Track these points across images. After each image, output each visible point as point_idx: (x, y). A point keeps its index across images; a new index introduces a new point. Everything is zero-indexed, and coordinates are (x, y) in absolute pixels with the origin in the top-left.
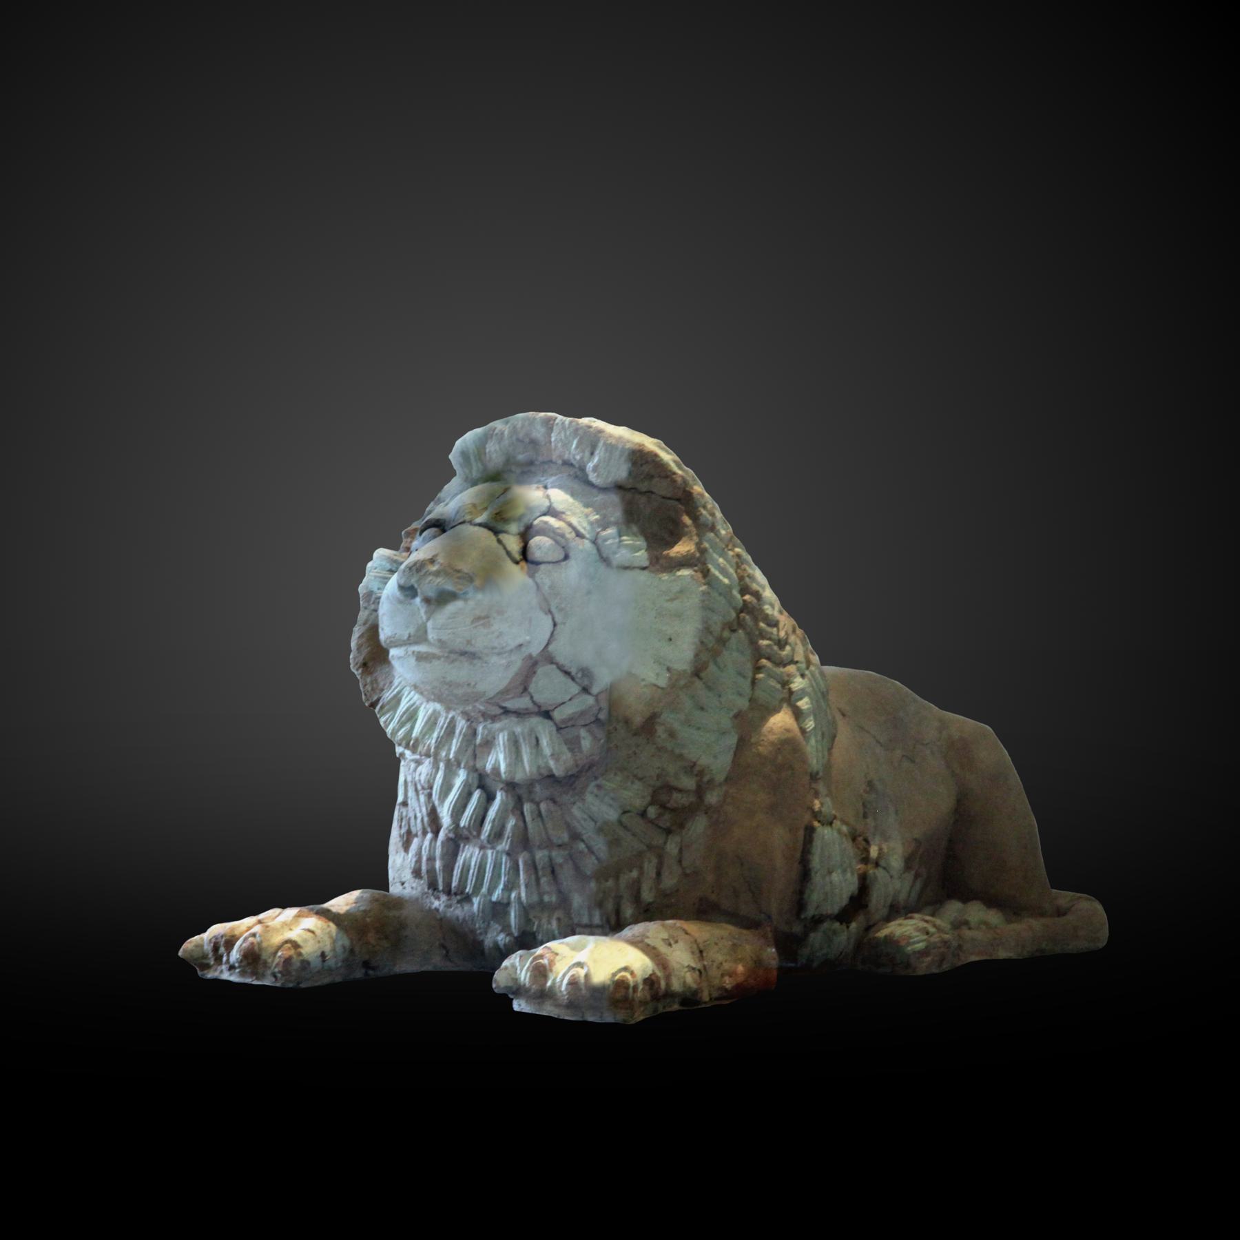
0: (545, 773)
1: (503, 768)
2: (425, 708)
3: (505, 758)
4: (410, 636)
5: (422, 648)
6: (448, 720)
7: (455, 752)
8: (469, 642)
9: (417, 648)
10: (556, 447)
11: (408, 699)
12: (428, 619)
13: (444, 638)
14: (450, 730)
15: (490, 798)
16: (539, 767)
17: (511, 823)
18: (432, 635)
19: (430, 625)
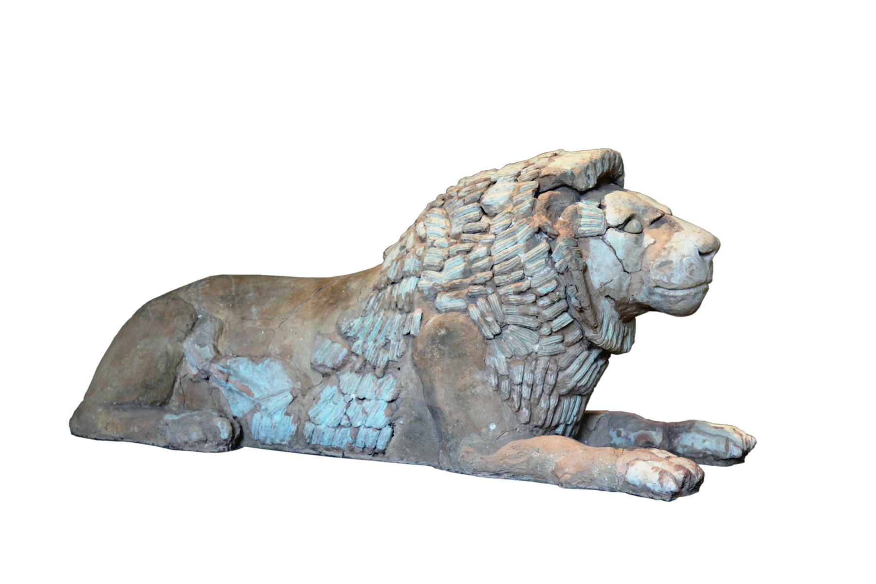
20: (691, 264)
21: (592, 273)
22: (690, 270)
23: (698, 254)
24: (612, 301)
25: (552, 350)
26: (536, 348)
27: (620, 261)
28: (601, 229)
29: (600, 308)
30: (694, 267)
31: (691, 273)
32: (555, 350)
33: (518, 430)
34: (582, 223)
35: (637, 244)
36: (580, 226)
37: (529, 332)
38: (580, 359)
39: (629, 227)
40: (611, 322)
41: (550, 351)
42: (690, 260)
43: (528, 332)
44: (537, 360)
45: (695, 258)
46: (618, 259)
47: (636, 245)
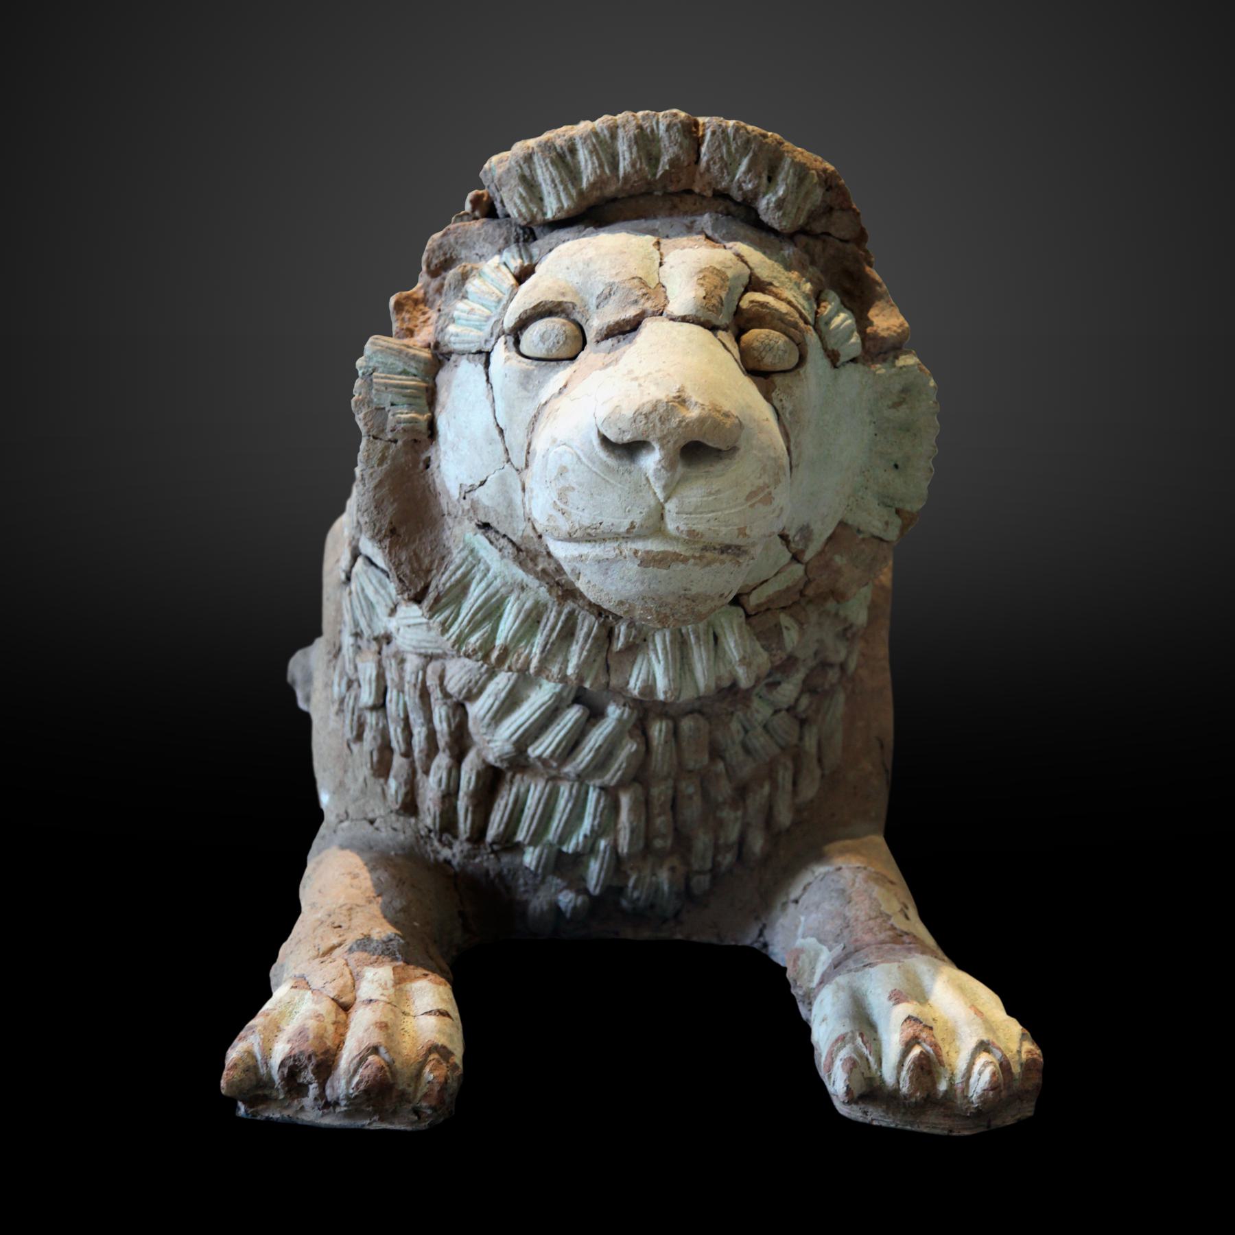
0: (726, 683)
1: (661, 684)
2: (518, 598)
3: (666, 669)
4: (632, 526)
5: (654, 546)
6: (563, 617)
7: (578, 666)
8: (742, 532)
9: (640, 546)
10: (708, 169)
11: (483, 584)
12: (667, 499)
13: (700, 527)
14: (568, 633)
15: (595, 714)
16: (719, 678)
17: (630, 747)
18: (672, 524)
19: (671, 507)
20: (563, 471)
21: (445, 453)
22: (562, 483)
23: (596, 441)
24: (503, 542)
25: (420, 641)
26: (392, 625)
27: (501, 431)
28: (481, 333)
29: (457, 557)
30: (572, 479)
31: (562, 494)
32: (427, 645)
33: (376, 824)
34: (456, 314)
35: (525, 389)
36: (453, 320)
37: (380, 581)
38: (498, 684)
39: (532, 337)
40: (512, 598)
41: (414, 643)
42: (561, 456)
43: (374, 581)
44: (402, 661)
45: (579, 452)
46: (498, 425)
47: (525, 393)
